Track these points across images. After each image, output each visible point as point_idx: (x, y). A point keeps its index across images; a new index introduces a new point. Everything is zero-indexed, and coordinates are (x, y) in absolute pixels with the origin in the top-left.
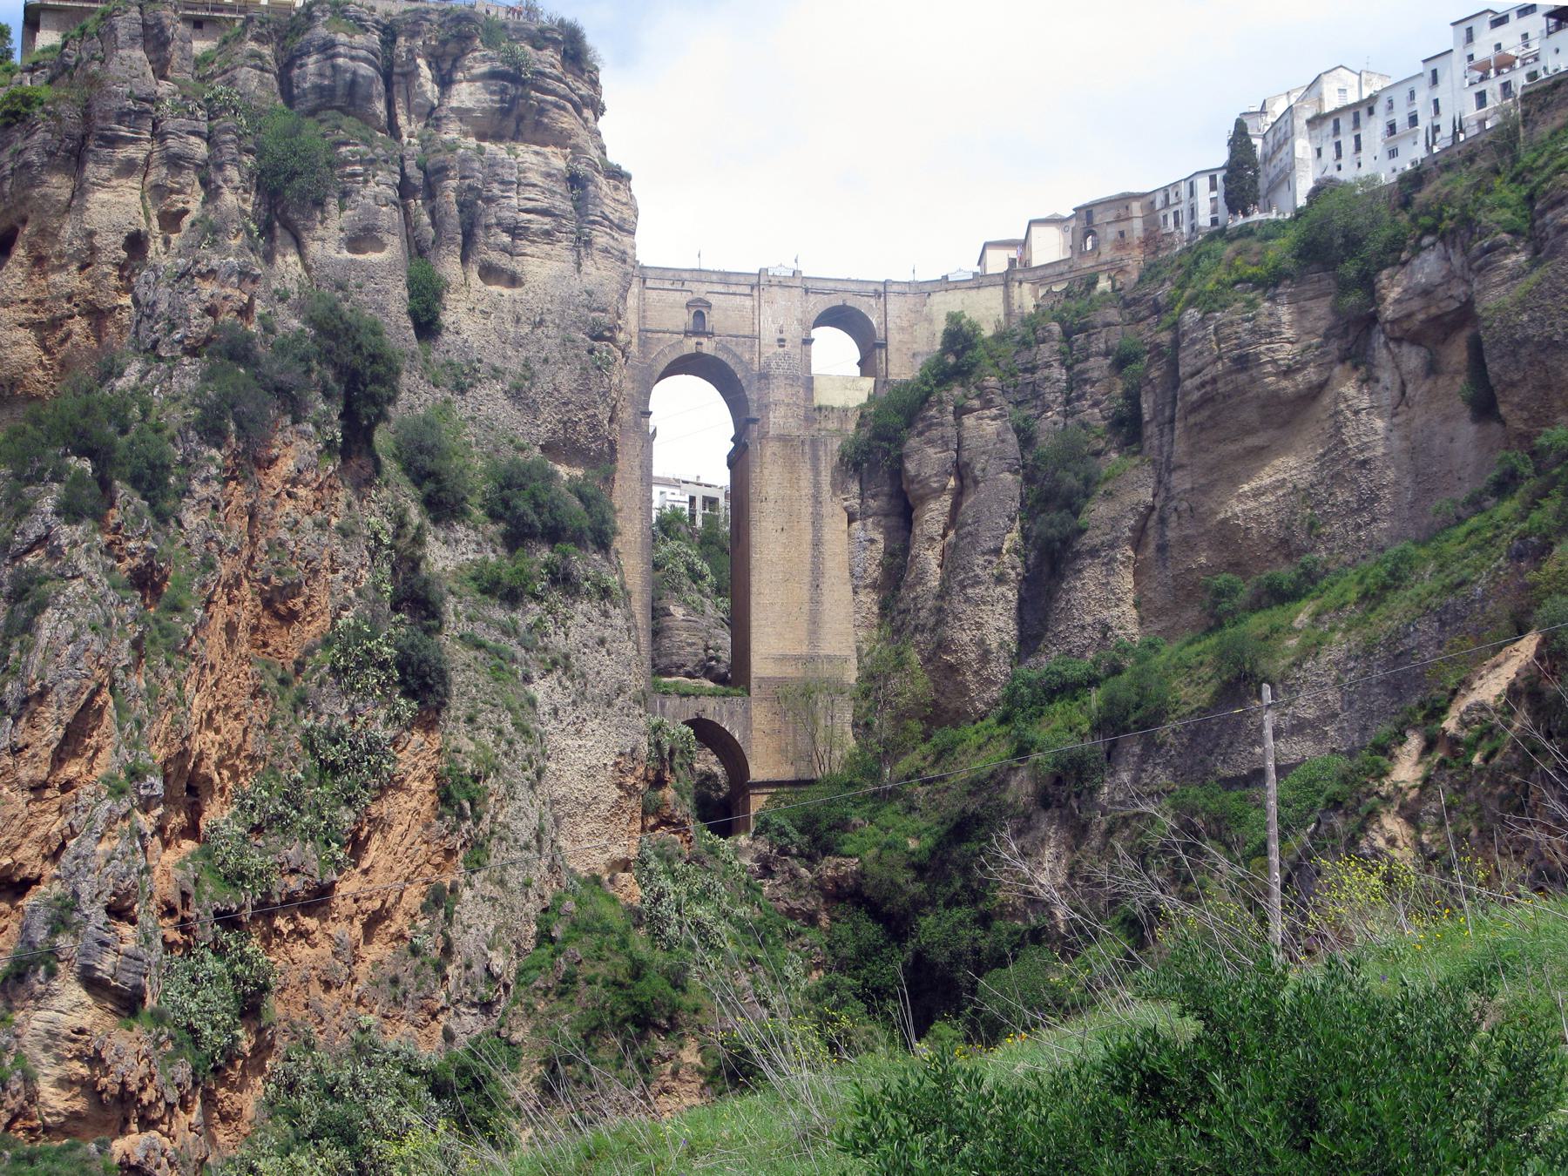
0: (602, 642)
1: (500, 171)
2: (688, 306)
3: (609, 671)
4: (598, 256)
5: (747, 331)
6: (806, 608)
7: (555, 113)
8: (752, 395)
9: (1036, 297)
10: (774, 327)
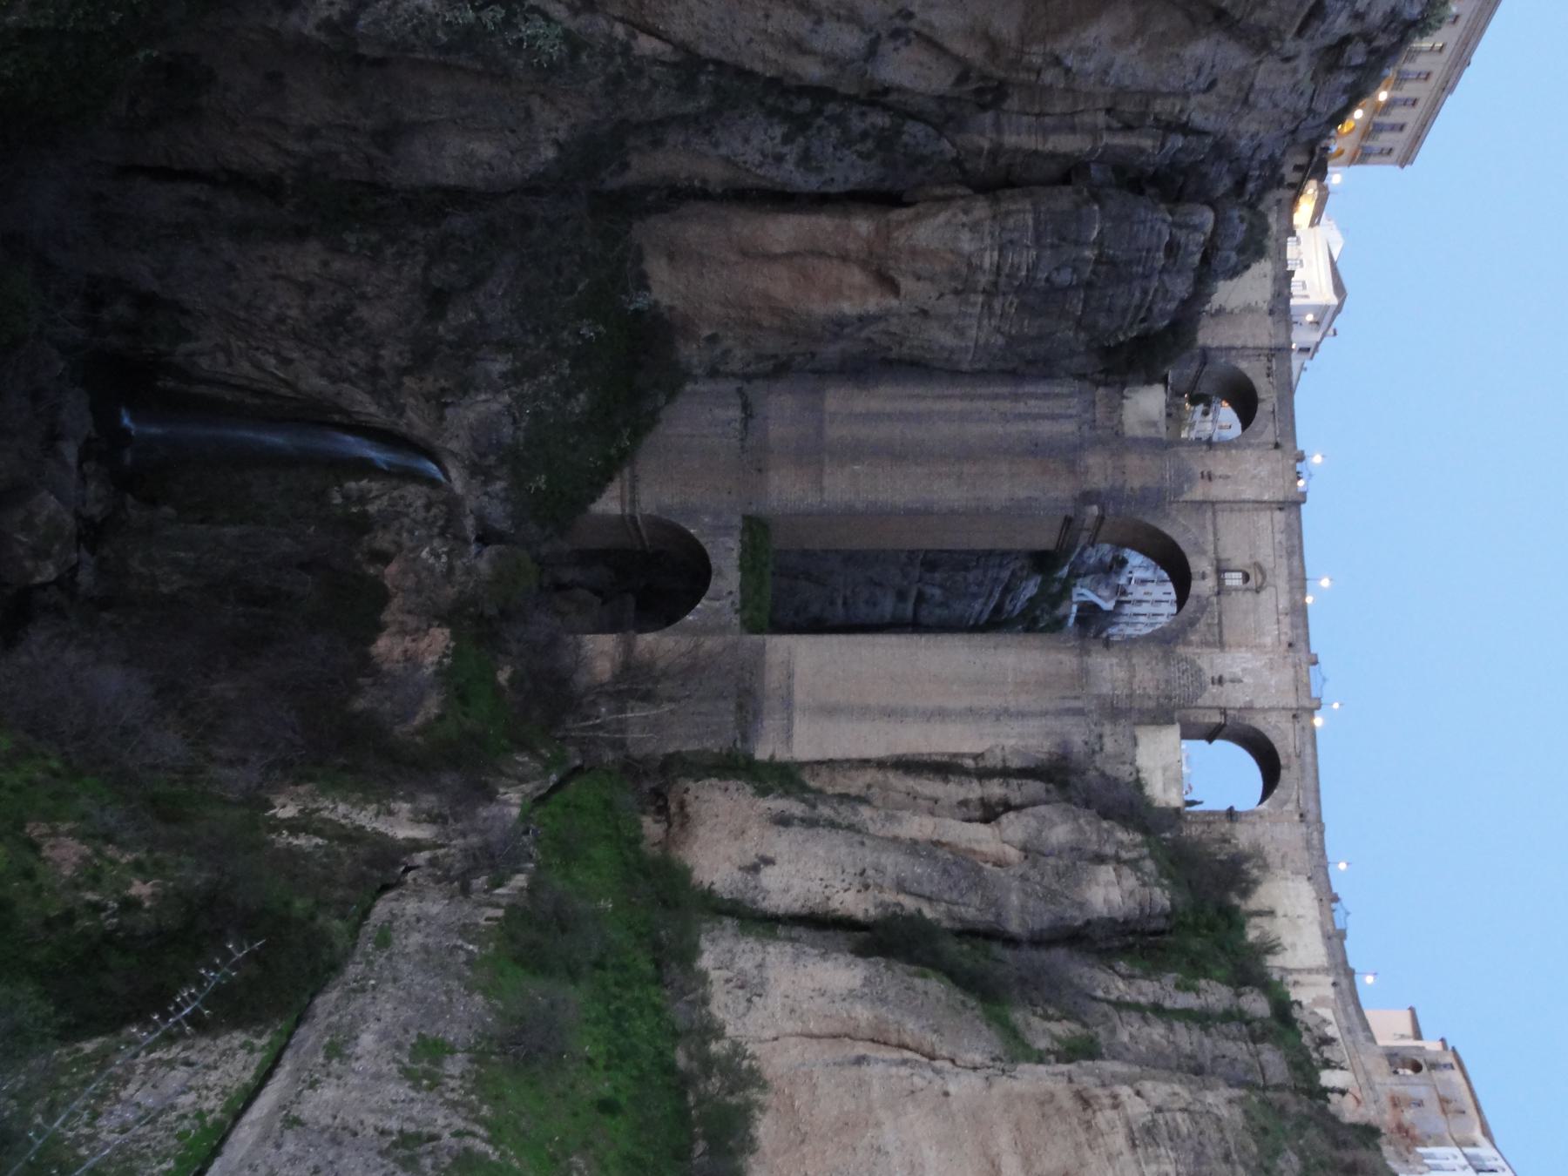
2: (1259, 567)
5: (1227, 637)
10: (1237, 671)
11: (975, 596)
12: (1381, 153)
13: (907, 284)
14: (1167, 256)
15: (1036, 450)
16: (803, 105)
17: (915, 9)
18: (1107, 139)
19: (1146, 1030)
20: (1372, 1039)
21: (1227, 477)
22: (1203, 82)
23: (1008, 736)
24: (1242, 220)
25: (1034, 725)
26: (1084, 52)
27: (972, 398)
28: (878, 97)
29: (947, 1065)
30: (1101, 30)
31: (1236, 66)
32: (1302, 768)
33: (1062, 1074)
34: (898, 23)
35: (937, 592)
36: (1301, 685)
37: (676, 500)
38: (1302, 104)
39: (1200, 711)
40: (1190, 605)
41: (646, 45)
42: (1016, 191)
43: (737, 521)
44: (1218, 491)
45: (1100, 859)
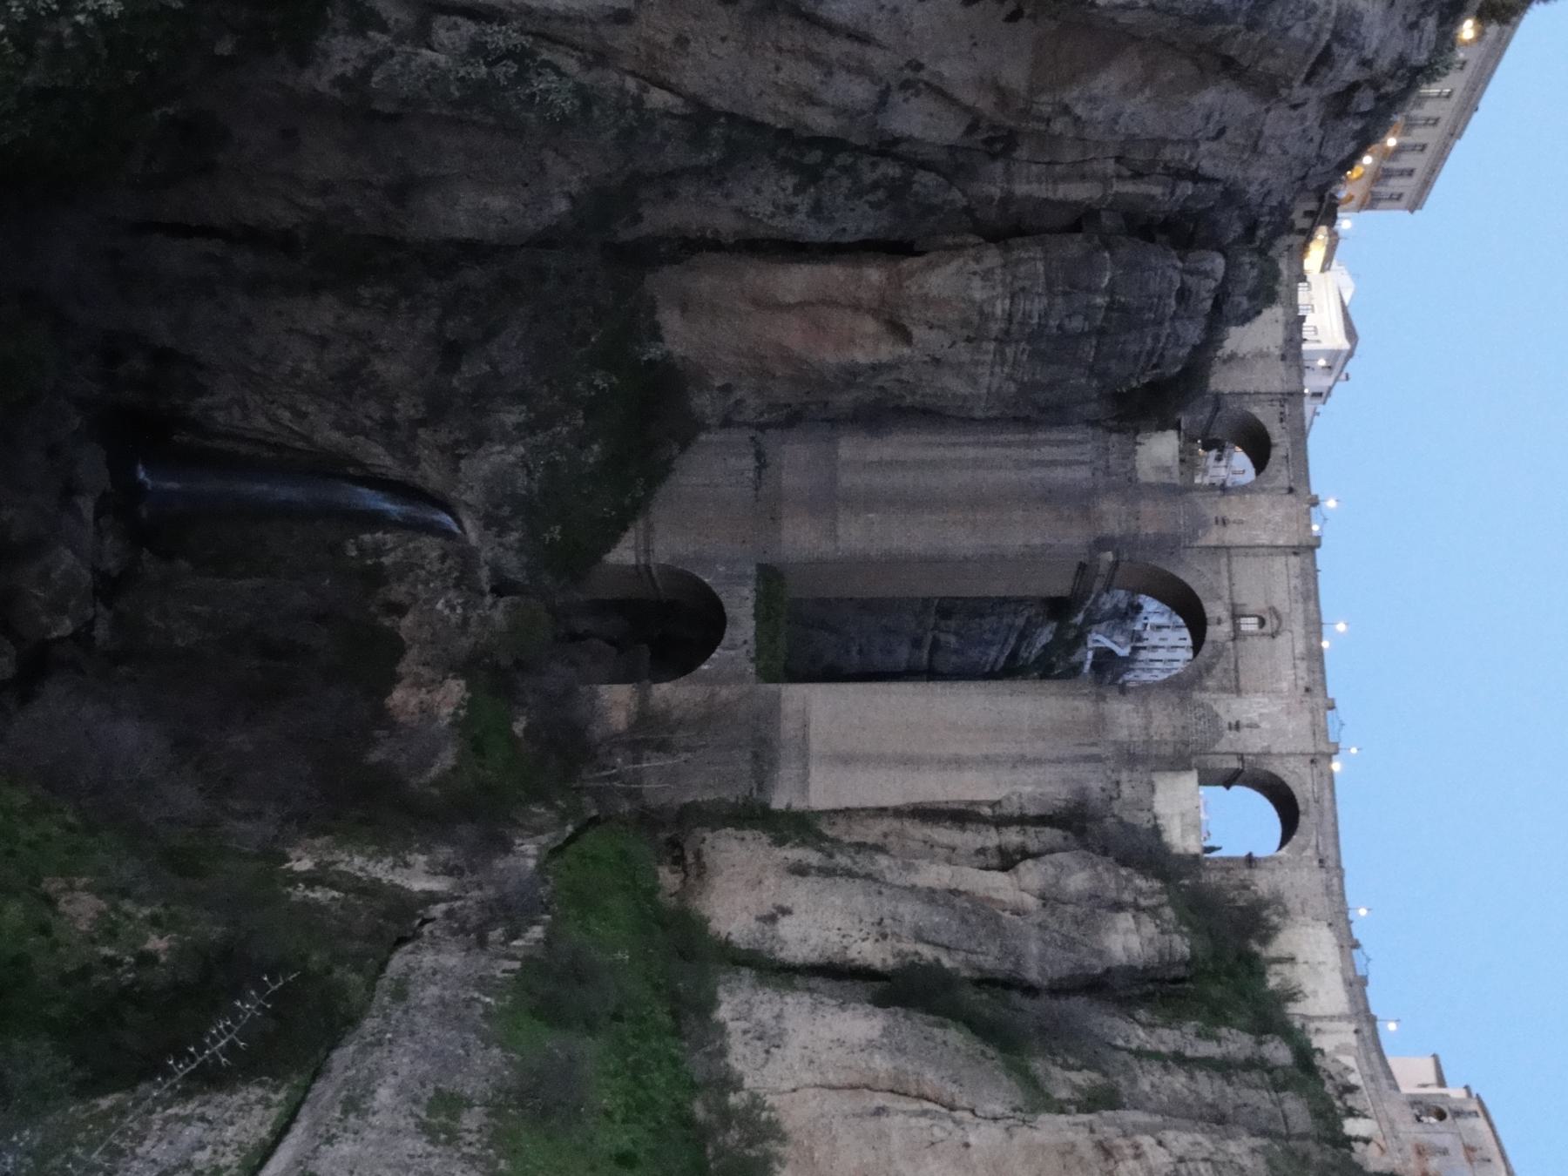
2: (1274, 611)
9: (1339, 1049)
10: (1254, 716)
11: (990, 644)
12: (1391, 198)
13: (918, 332)
14: (1179, 303)
15: (1050, 497)
16: (815, 156)
17: (924, 60)
18: (1119, 187)
19: (1167, 1078)
20: (1396, 1088)
21: (1241, 522)
22: (1212, 129)
23: (1025, 784)
24: (1253, 265)
25: (1051, 772)
26: (1092, 100)
27: (985, 445)
28: (888, 147)
29: (967, 1115)
30: (1108, 81)
31: (1246, 113)
32: (1321, 814)
33: (1084, 1124)
34: (908, 74)
35: (952, 639)
36: (1318, 730)
37: (691, 548)
38: (1312, 150)
39: (1219, 757)
40: (1206, 649)
41: (657, 98)
42: (1027, 240)
43: (751, 570)
44: (1233, 536)
45: (1118, 907)
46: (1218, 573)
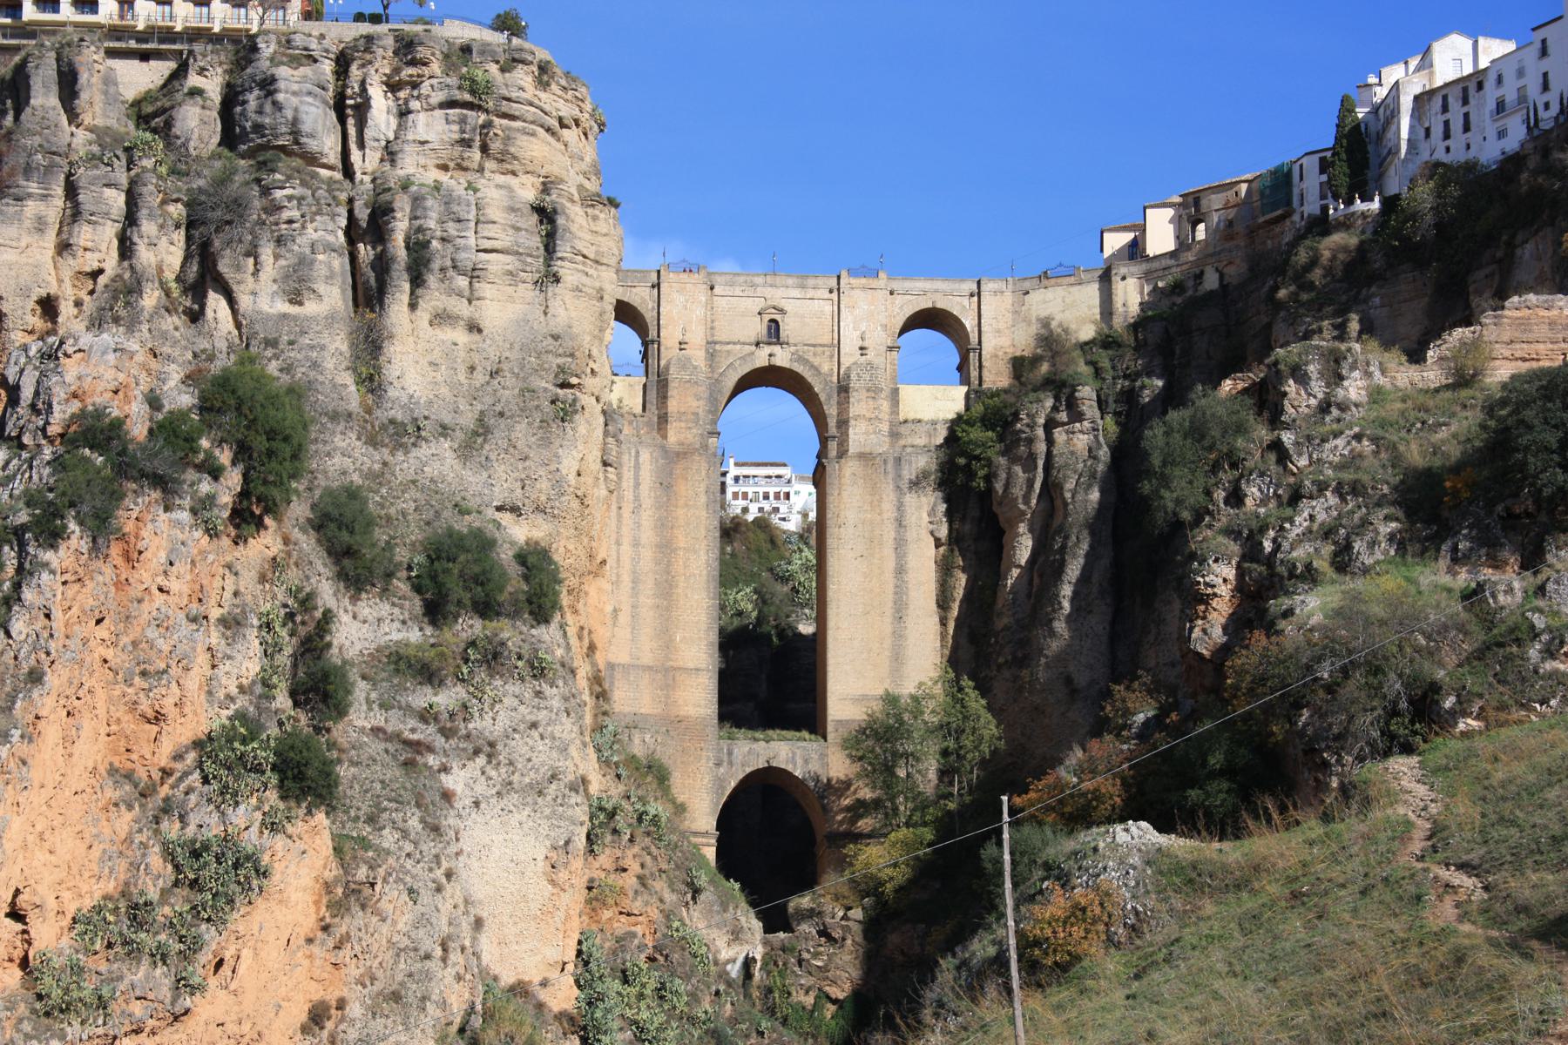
0: (534, 725)
1: (455, 208)
3: (543, 757)
4: (568, 297)
6: (888, 643)
7: (523, 141)
8: (831, 411)
15: (666, 485)
21: (684, 329)
23: (921, 518)
44: (697, 337)
46: (729, 352)
